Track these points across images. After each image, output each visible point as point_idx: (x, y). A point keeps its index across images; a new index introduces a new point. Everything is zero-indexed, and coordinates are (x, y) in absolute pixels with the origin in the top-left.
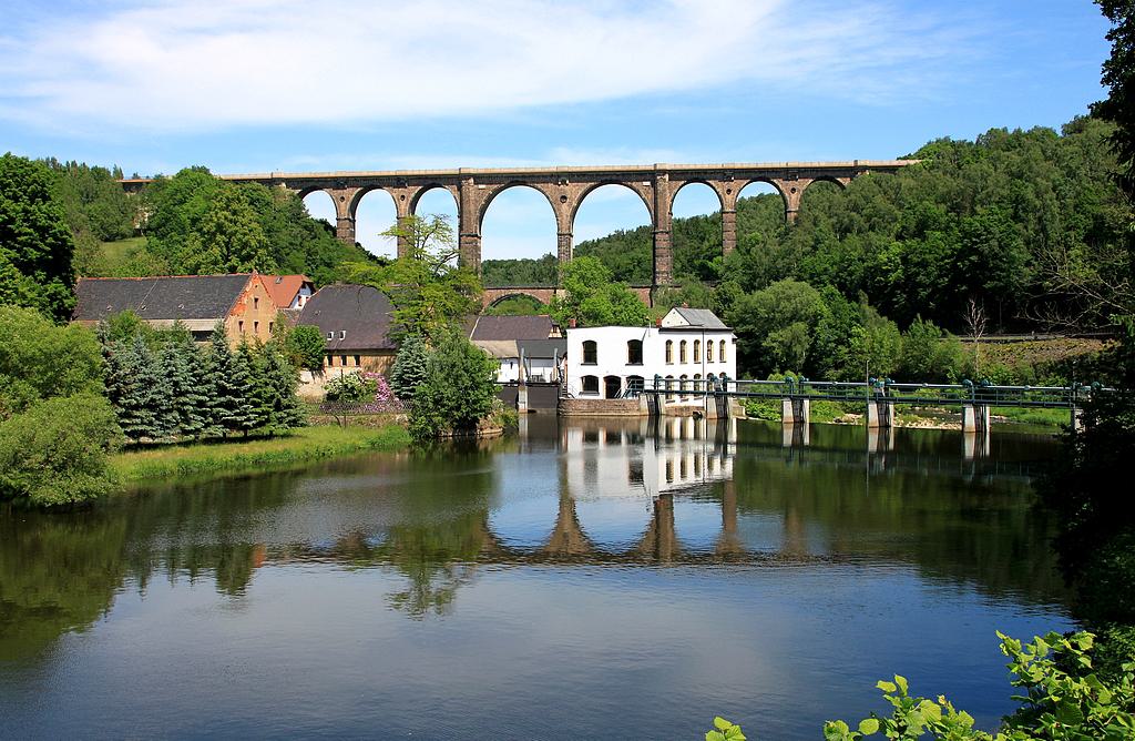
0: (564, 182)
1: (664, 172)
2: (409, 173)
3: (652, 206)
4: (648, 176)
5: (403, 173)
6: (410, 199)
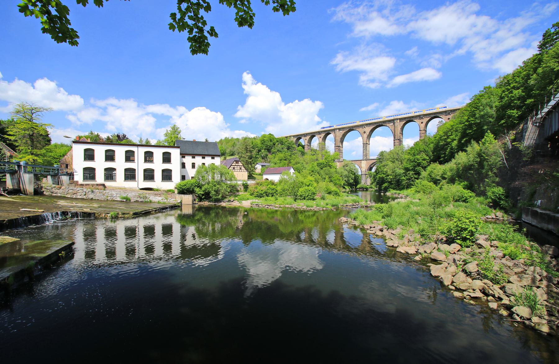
0: (364, 127)
1: (397, 119)
3: (393, 132)
4: (392, 122)
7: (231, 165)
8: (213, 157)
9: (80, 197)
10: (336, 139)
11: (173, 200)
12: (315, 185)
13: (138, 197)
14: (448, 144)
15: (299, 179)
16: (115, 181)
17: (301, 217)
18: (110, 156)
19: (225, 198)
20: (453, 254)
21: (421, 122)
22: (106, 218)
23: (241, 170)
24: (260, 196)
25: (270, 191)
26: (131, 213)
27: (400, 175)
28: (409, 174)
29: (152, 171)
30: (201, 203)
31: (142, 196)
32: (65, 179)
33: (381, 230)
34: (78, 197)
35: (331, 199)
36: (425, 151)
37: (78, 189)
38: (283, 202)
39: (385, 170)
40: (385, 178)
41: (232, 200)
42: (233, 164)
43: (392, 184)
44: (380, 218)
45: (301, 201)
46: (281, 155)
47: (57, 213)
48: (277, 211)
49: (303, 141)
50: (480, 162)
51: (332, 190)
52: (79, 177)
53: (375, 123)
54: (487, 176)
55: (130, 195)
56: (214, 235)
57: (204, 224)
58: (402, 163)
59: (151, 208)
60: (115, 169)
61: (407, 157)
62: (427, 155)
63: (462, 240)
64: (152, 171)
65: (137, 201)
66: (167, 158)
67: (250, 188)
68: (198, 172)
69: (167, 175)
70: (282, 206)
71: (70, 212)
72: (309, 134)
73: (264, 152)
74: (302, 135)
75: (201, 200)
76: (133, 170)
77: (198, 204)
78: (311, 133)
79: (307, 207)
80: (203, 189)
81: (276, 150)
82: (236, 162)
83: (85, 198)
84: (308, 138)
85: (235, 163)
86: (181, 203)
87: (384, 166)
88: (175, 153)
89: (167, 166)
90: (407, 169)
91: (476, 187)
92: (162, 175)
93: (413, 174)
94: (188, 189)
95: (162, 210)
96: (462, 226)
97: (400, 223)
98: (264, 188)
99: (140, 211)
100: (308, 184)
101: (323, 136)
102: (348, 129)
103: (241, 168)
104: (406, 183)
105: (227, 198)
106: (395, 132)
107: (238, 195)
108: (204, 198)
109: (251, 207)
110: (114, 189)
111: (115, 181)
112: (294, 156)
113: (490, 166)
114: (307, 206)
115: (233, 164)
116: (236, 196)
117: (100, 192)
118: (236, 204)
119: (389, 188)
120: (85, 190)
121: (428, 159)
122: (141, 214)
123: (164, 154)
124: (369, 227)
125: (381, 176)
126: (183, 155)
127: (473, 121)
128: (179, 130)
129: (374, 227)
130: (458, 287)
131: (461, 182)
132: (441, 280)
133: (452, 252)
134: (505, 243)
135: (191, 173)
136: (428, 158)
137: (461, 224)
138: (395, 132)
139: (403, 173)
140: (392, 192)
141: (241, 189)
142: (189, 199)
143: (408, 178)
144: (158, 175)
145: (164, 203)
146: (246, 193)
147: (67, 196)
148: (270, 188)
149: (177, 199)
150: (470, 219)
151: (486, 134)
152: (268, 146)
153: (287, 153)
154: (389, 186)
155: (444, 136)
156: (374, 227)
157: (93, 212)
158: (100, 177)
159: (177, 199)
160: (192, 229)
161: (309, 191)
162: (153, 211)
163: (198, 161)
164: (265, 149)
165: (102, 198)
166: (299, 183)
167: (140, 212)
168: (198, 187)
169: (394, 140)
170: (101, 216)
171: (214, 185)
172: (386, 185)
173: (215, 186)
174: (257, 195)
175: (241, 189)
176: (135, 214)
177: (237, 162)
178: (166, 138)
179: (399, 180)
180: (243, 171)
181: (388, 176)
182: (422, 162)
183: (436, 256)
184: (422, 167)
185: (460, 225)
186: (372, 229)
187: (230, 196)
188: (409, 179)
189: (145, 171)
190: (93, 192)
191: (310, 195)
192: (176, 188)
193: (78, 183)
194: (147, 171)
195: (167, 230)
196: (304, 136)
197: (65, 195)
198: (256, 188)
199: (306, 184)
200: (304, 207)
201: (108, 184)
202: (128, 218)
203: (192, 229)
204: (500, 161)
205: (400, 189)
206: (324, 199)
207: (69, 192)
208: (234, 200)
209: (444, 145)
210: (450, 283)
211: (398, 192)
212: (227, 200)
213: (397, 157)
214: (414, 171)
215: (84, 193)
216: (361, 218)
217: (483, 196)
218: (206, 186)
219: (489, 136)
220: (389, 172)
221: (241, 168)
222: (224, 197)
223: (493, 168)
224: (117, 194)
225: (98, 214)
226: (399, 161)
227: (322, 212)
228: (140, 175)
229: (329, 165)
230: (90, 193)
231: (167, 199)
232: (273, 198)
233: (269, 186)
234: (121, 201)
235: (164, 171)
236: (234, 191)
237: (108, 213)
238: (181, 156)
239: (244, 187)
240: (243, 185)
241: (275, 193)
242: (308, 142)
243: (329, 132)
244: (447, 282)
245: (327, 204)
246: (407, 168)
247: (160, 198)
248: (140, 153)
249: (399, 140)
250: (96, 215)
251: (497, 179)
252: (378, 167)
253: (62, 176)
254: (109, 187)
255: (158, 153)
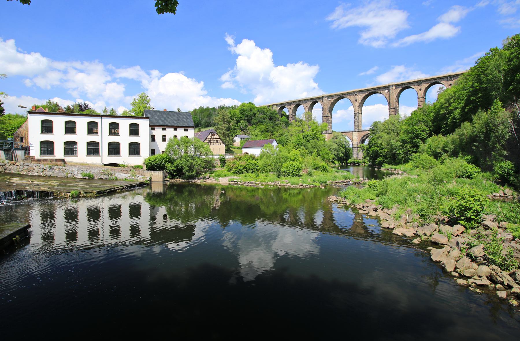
0: (356, 95)
1: (392, 86)
2: (308, 98)
3: (388, 99)
4: (387, 88)
5: (306, 98)
6: (309, 107)
7: (207, 138)
8: (186, 129)
9: (37, 174)
10: (324, 107)
11: (141, 177)
12: (301, 159)
13: (103, 173)
14: (451, 112)
15: (283, 154)
16: (76, 156)
17: (285, 196)
18: (70, 128)
19: (200, 174)
20: (456, 236)
21: (420, 88)
22: (66, 197)
23: (217, 144)
24: (239, 172)
25: (250, 167)
26: (95, 192)
27: (397, 148)
28: (406, 147)
29: (118, 144)
30: (173, 180)
31: (106, 173)
32: (19, 154)
33: (375, 210)
34: (35, 174)
35: (319, 175)
36: (425, 121)
37: (34, 165)
38: (265, 179)
39: (379, 142)
40: (380, 151)
41: (208, 177)
42: (209, 137)
43: (388, 158)
44: (374, 196)
45: (285, 177)
46: (263, 126)
47: (11, 192)
48: (258, 189)
49: (286, 111)
50: (486, 132)
51: (320, 165)
52: (35, 152)
53: (368, 90)
54: (494, 148)
55: (94, 172)
56: (187, 216)
57: (176, 204)
58: (398, 134)
59: (116, 187)
60: (76, 143)
61: (404, 127)
62: (427, 126)
63: (466, 221)
64: (118, 144)
65: (101, 178)
66: (134, 130)
67: (228, 163)
68: (170, 146)
69: (134, 149)
70: (263, 183)
71: (25, 191)
72: (293, 102)
73: (243, 123)
74: (286, 104)
75: (172, 176)
76: (97, 144)
77: (170, 181)
78: (296, 102)
79: (292, 184)
80: (175, 164)
81: (256, 121)
82: (212, 134)
83: (43, 175)
84: (292, 107)
85: (211, 135)
86: (150, 180)
87: (378, 138)
88: (144, 125)
89: (134, 139)
90: (404, 142)
91: (482, 161)
92: (129, 149)
93: (410, 147)
94: (158, 164)
95: (130, 188)
96: (466, 205)
97: (396, 202)
98: (243, 163)
99: (104, 189)
100: (293, 158)
101: (309, 105)
102: (337, 97)
103: (217, 141)
104: (403, 157)
105: (202, 174)
106: (390, 99)
107: (214, 171)
108: (176, 175)
109: (229, 184)
110: (75, 165)
111: (76, 156)
112: (277, 128)
113: (497, 137)
114: (292, 184)
115: (209, 137)
116: (212, 172)
117: (59, 169)
118: (212, 181)
119: (384, 163)
120: (42, 166)
121: (428, 130)
122: (106, 192)
123: (131, 125)
124: (361, 207)
125: (375, 149)
126: (152, 127)
127: (477, 86)
128: (148, 98)
129: (367, 207)
130: (462, 274)
131: (465, 156)
132: (443, 266)
133: (455, 235)
134: (515, 224)
135: (161, 146)
136: (428, 129)
137: (465, 202)
138: (390, 102)
139: (400, 146)
140: (387, 167)
141: (217, 164)
142: (160, 176)
143: (405, 151)
144: (124, 149)
145: (131, 181)
146: (223, 169)
147: (22, 173)
148: (250, 163)
149: (146, 175)
150: (475, 198)
151: (495, 101)
152: (248, 116)
153: (269, 124)
154: (384, 161)
155: (445, 103)
156: (367, 207)
157: (51, 191)
158: (59, 152)
159: (146, 175)
160: (162, 210)
161: (294, 166)
162: (118, 189)
163: (170, 133)
164: (244, 120)
165: (62, 175)
166: (283, 158)
167: (105, 191)
168: (169, 162)
169: (389, 109)
170: (60, 196)
171: (187, 160)
172: (380, 159)
173: (188, 161)
174: (236, 171)
175: (217, 164)
176: (98, 193)
177: (213, 134)
178: (133, 107)
179: (395, 154)
180: (220, 144)
181: (383, 149)
182: (421, 133)
183: (437, 238)
184: (421, 139)
185: (464, 204)
186: (365, 209)
187: (205, 172)
188: (406, 153)
189: (110, 144)
190: (51, 168)
191: (295, 170)
192: (144, 164)
193: (34, 158)
194: (112, 144)
195: (135, 211)
196: (288, 104)
197: (20, 172)
198: (235, 163)
199: (291, 159)
200: (288, 185)
201: (69, 159)
202: (91, 198)
203: (162, 210)
204: (509, 132)
205: (397, 164)
206: (311, 175)
207: (24, 169)
208: (210, 177)
209: (445, 114)
210: (453, 270)
211: (394, 167)
212: (202, 176)
213: (393, 128)
214: (411, 144)
215: (42, 170)
216: (352, 196)
217: (490, 171)
218: (178, 161)
219: (498, 103)
220: (384, 145)
221: (217, 141)
222: (198, 174)
223: (501, 139)
224: (78, 171)
225: (57, 193)
226: (394, 132)
227: (309, 190)
228: (104, 149)
229: (316, 137)
230: (48, 169)
231: (134, 176)
232: (254, 175)
233: (249, 161)
234: (83, 178)
235: (131, 144)
236: (209, 166)
237: (69, 191)
238: (150, 128)
239: (221, 162)
240: (220, 160)
241: (256, 168)
242: (292, 112)
243: (316, 100)
244: (449, 268)
245: (314, 181)
246: (404, 140)
247: (127, 175)
248: (104, 124)
249: (394, 108)
250: (55, 194)
251: (505, 153)
252: (371, 139)
253: (17, 151)
254: (69, 162)
255: (124, 125)
